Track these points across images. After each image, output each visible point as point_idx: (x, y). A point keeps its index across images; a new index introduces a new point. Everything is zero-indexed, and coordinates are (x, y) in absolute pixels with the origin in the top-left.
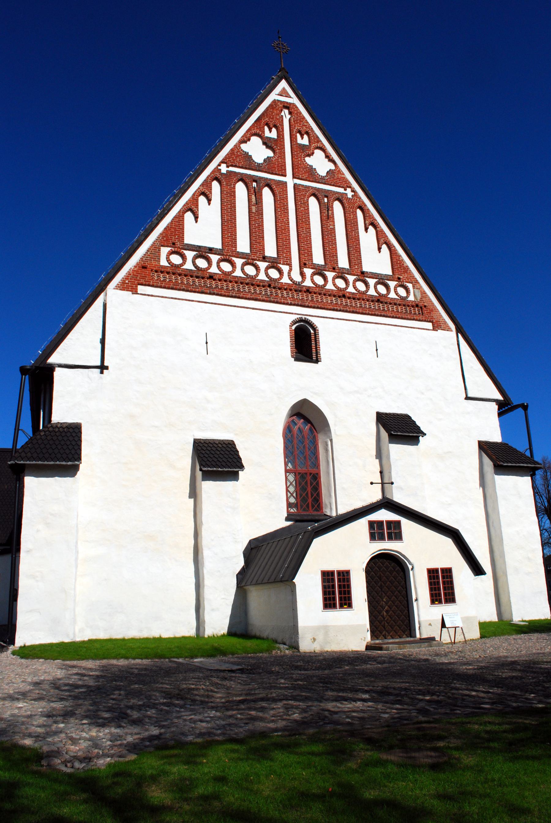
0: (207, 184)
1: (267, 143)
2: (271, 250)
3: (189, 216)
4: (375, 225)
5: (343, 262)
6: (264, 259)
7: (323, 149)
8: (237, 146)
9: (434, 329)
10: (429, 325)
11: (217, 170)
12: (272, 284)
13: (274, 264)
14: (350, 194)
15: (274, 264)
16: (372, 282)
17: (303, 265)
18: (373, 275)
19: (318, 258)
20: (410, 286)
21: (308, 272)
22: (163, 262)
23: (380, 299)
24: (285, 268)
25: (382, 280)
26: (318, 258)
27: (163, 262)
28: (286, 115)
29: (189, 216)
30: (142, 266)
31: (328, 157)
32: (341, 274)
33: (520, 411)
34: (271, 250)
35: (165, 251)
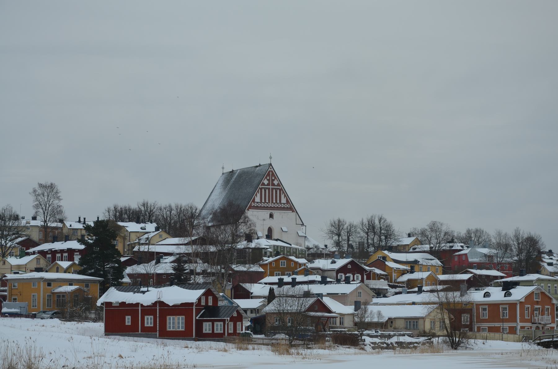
0: (258, 191)
1: (268, 180)
2: (267, 201)
3: (256, 196)
4: (284, 194)
5: (278, 202)
6: (266, 203)
7: (277, 179)
8: (263, 182)
9: (292, 212)
10: (291, 211)
11: (260, 187)
12: (267, 207)
13: (267, 203)
14: (280, 188)
15: (267, 203)
16: (282, 204)
17: (272, 203)
18: (283, 203)
19: (274, 202)
20: (289, 204)
21: (273, 204)
22: (252, 205)
23: (284, 208)
24: (269, 204)
25: (284, 204)
26: (274, 202)
27: (252, 205)
28: (271, 173)
29: (256, 196)
30: (250, 206)
31: (277, 180)
32: (278, 203)
33: (305, 226)
34: (267, 201)
35: (252, 203)
